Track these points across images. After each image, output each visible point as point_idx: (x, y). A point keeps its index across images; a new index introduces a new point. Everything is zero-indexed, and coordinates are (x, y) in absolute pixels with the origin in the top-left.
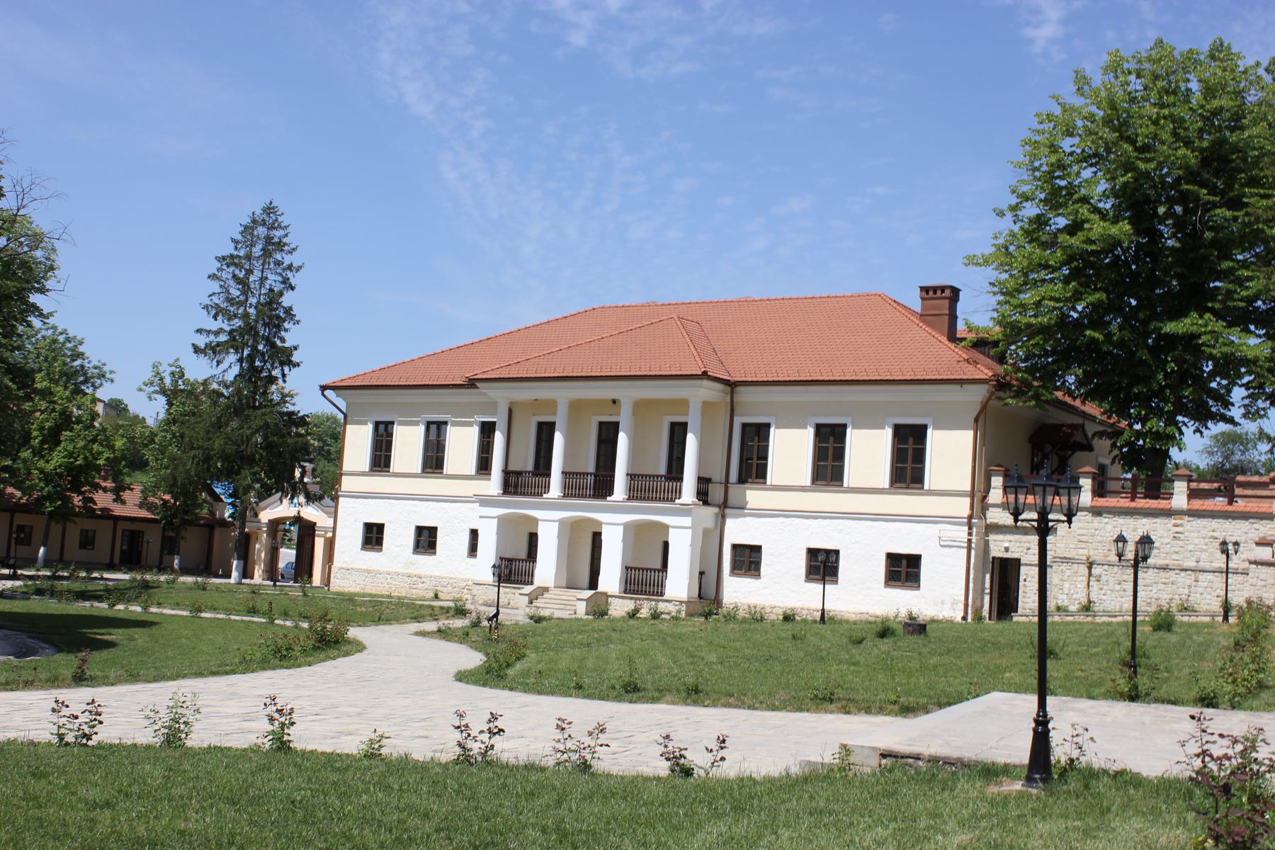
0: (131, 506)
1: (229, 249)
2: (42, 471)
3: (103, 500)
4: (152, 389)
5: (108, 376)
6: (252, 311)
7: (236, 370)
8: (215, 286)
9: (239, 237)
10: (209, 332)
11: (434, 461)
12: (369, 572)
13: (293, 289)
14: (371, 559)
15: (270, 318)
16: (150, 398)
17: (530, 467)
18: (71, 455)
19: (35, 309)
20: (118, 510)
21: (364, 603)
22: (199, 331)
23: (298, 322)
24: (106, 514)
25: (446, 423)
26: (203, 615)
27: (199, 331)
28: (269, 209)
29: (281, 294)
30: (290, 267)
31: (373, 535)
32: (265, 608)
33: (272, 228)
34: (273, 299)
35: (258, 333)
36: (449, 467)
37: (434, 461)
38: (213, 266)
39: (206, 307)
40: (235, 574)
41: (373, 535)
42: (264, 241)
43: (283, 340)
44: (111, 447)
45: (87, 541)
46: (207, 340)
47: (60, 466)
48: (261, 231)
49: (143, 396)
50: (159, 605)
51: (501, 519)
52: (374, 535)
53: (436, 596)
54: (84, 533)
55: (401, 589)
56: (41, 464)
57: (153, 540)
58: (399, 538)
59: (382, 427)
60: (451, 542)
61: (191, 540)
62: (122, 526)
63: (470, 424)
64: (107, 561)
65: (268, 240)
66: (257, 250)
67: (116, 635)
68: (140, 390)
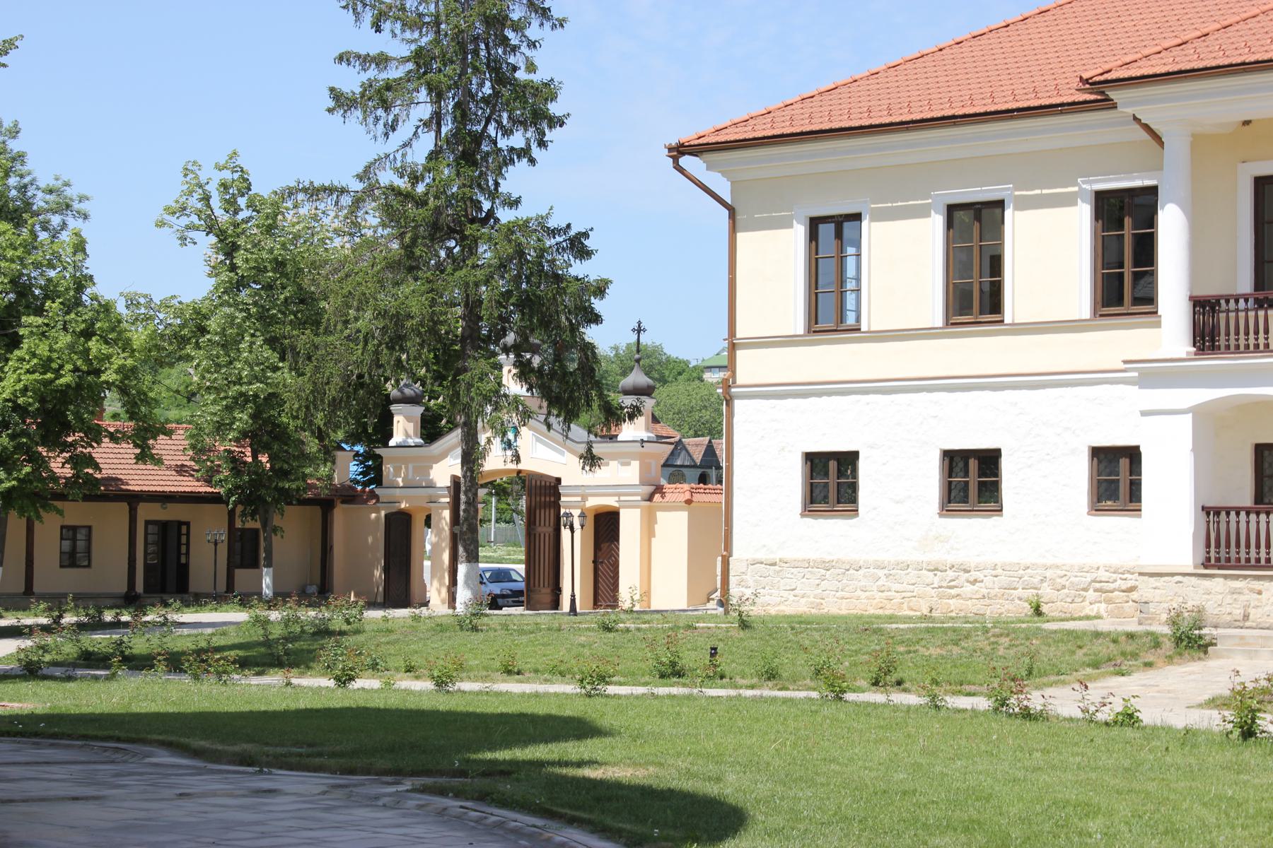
0: (167, 470)
3: (114, 460)
4: (184, 221)
5: (76, 206)
7: (427, 142)
11: (976, 293)
12: (827, 565)
14: (830, 533)
16: (183, 239)
17: (1245, 284)
18: (46, 365)
20: (141, 479)
23: (561, 23)
24: (113, 493)
25: (1000, 204)
26: (612, 690)
31: (832, 480)
36: (1015, 305)
37: (976, 293)
41: (832, 480)
43: (531, 68)
44: (127, 346)
45: (76, 553)
46: (364, 77)
47: (26, 389)
49: (168, 237)
51: (1201, 414)
53: (1038, 611)
54: (70, 532)
55: (907, 599)
58: (899, 482)
59: (826, 231)
60: (1049, 479)
61: (290, 533)
63: (1068, 201)
64: (123, 588)
68: (161, 224)
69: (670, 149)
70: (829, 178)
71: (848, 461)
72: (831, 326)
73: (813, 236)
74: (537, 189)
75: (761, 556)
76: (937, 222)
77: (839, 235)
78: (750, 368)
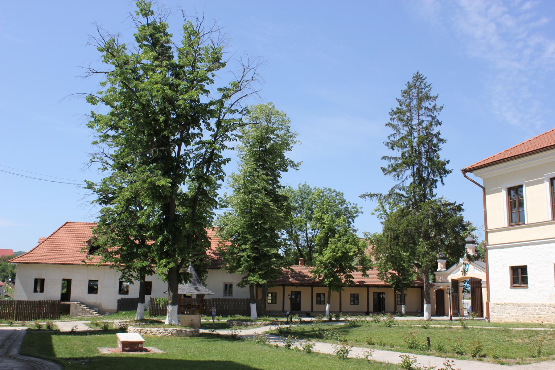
2: (321, 262)
3: (357, 276)
4: (379, 213)
7: (411, 180)
9: (400, 98)
10: (390, 158)
12: (519, 305)
13: (440, 124)
14: (519, 294)
21: (518, 334)
22: (384, 158)
24: (362, 285)
27: (384, 158)
28: (418, 78)
31: (519, 275)
35: (422, 158)
39: (387, 144)
40: (426, 314)
41: (519, 275)
46: (390, 163)
47: (329, 258)
52: (520, 276)
56: (320, 258)
57: (389, 298)
59: (512, 192)
61: (411, 295)
62: (372, 290)
64: (366, 310)
66: (415, 103)
68: (373, 214)
69: (462, 171)
70: (510, 174)
71: (524, 269)
72: (517, 223)
73: (509, 194)
74: (446, 191)
75: (499, 302)
76: (546, 185)
77: (517, 193)
78: (493, 239)
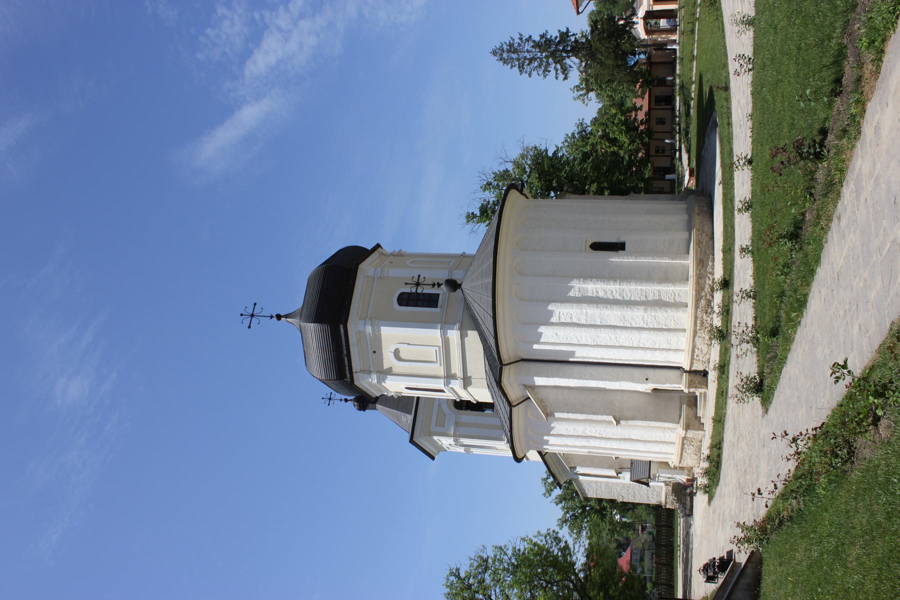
0: (643, 103)
1: (516, 69)
2: (629, 145)
3: (641, 116)
6: (544, 54)
7: (573, 58)
8: (534, 73)
9: (510, 65)
10: (557, 74)
13: (530, 37)
15: (546, 45)
18: (621, 132)
19: (555, 153)
20: (646, 108)
22: (557, 78)
27: (557, 78)
28: (494, 53)
29: (534, 41)
30: (521, 39)
32: (691, 25)
33: (503, 50)
34: (537, 45)
35: (554, 50)
38: (525, 75)
39: (545, 76)
40: (674, 47)
42: (510, 54)
43: (556, 37)
44: (616, 115)
45: (661, 122)
48: (505, 55)
50: (691, 78)
54: (657, 123)
56: (626, 145)
57: (659, 91)
61: (658, 72)
62: (653, 106)
65: (509, 51)
66: (514, 56)
67: (706, 89)
